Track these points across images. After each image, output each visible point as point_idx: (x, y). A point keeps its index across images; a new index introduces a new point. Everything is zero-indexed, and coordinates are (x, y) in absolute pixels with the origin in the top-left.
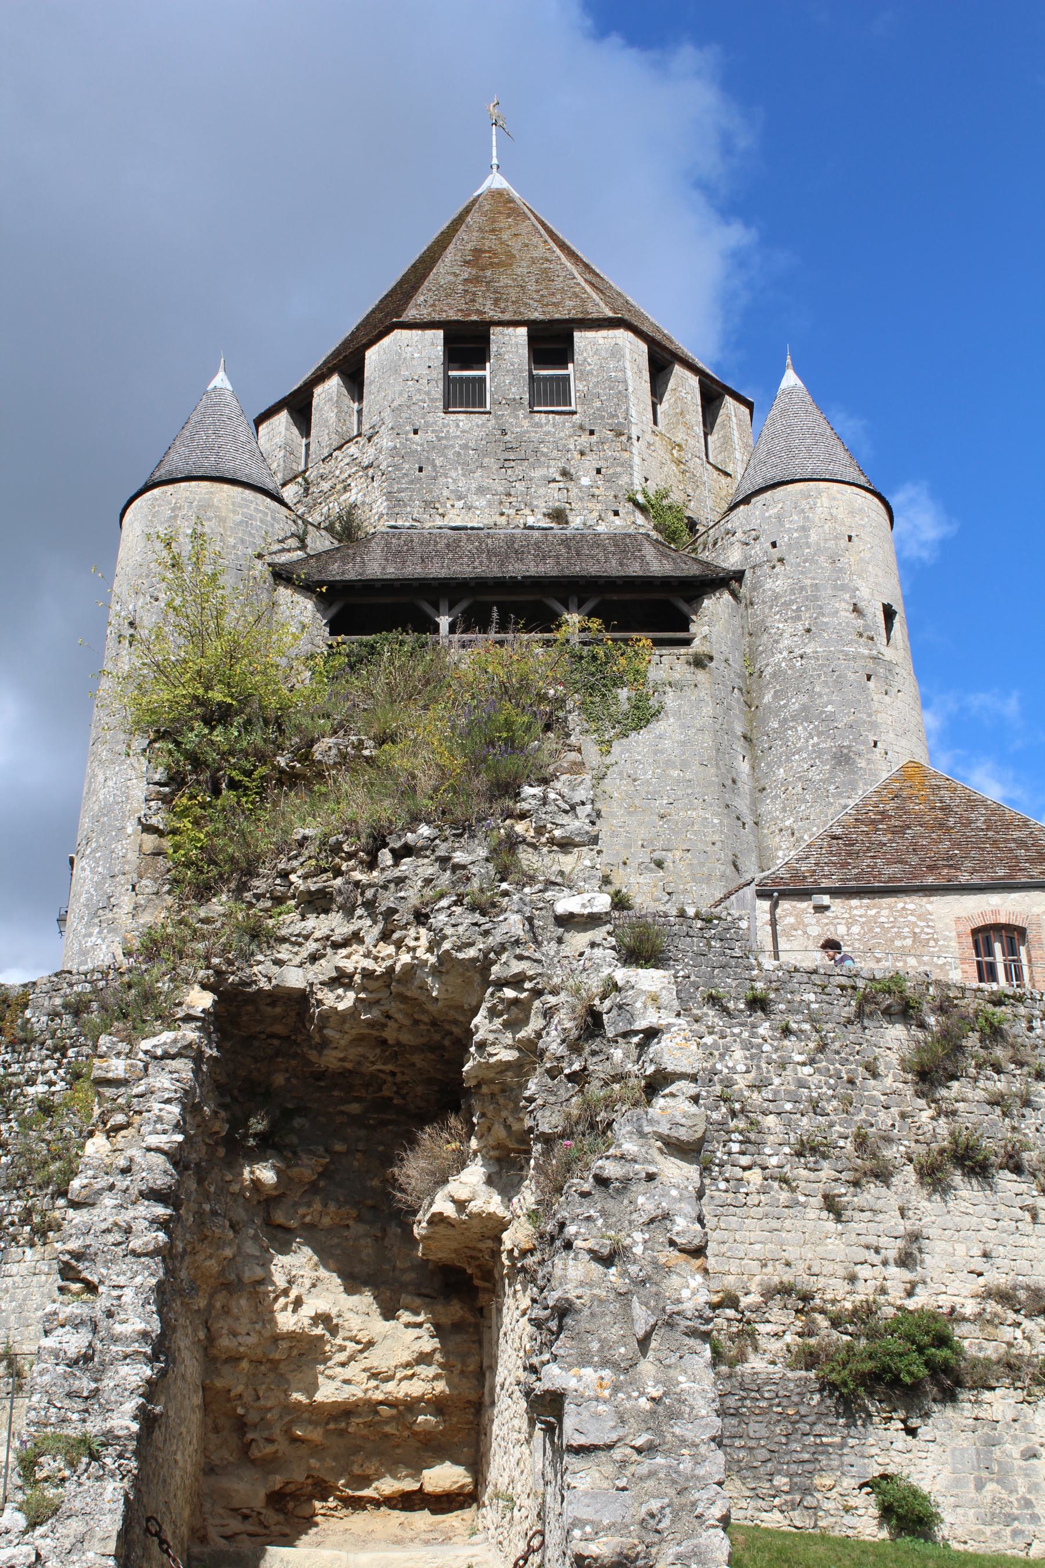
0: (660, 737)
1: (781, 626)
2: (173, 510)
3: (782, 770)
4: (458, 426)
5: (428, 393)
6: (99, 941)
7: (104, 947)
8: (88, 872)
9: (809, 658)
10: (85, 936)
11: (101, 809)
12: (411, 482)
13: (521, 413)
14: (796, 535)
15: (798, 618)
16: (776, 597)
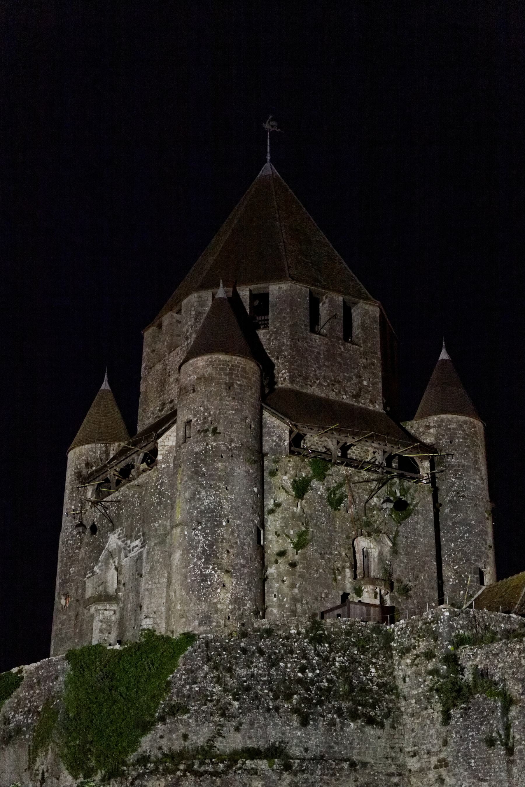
0: (417, 523)
1: (454, 480)
2: (230, 369)
3: (453, 545)
4: (316, 341)
5: (304, 321)
6: (213, 572)
7: (216, 576)
8: (201, 537)
9: (467, 498)
10: (203, 568)
11: (205, 508)
12: (298, 366)
13: (340, 342)
14: (461, 440)
15: (460, 478)
16: (453, 466)
